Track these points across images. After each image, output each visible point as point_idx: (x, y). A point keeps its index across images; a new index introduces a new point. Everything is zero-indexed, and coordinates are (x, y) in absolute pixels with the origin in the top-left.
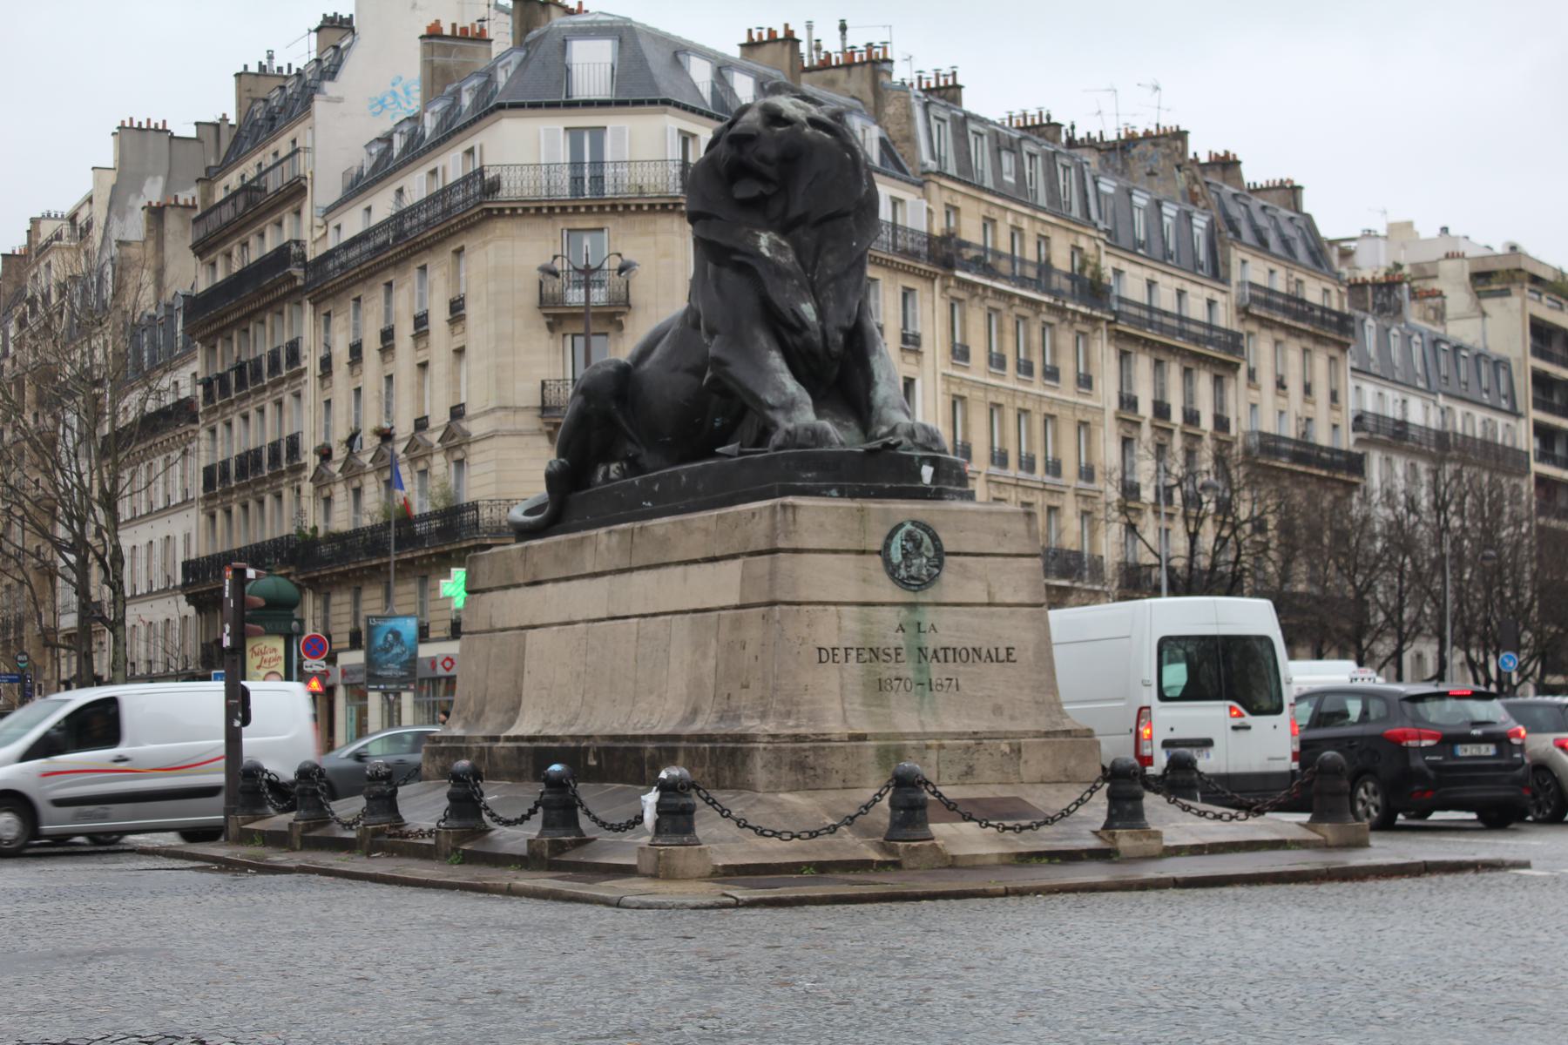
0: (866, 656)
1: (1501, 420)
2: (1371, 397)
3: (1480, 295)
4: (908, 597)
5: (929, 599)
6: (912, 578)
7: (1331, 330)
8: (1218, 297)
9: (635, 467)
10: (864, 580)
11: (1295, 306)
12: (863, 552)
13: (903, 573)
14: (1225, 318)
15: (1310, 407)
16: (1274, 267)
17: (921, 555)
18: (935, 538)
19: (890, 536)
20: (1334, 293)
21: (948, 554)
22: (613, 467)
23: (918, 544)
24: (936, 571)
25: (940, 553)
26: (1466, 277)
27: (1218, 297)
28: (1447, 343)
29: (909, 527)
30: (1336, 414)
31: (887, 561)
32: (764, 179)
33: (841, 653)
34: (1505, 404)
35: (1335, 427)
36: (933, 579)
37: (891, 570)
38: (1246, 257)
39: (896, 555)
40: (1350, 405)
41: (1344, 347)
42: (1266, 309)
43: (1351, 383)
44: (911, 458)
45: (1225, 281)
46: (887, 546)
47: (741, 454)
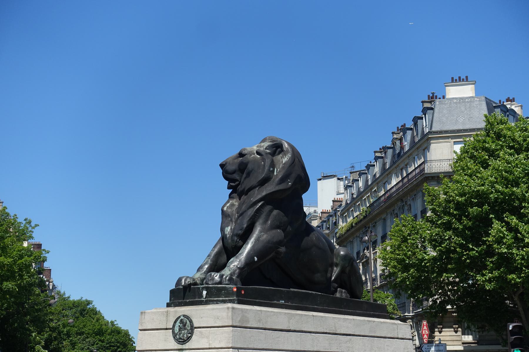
4: (180, 347)
5: (187, 348)
6: (180, 338)
10: (165, 341)
12: (167, 329)
13: (178, 336)
17: (185, 329)
18: (191, 321)
19: (175, 322)
21: (196, 328)
23: (185, 325)
24: (190, 335)
25: (193, 328)
29: (182, 317)
31: (173, 332)
36: (189, 339)
37: (174, 335)
39: (177, 329)
44: (199, 288)
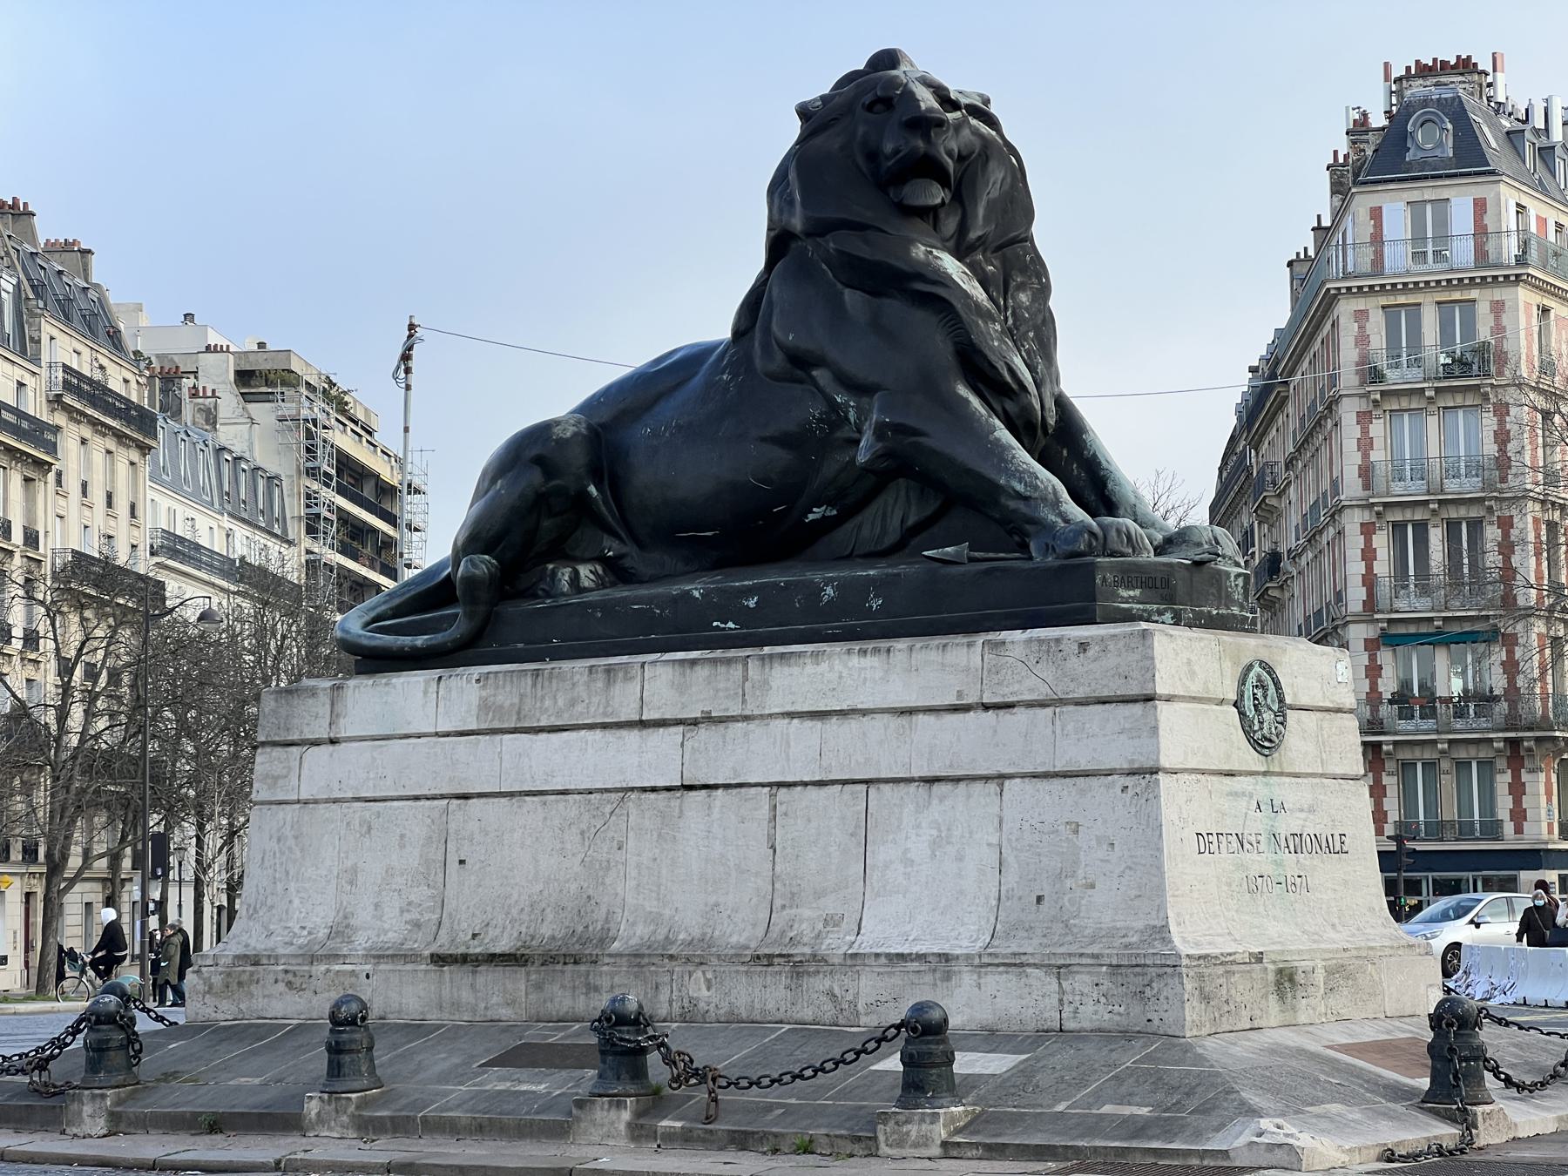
0: (1235, 844)
1: (275, 547)
2: (169, 511)
3: (247, 398)
7: (133, 425)
8: (28, 379)
9: (617, 572)
11: (97, 394)
14: (35, 406)
15: (112, 522)
16: (80, 347)
18: (1277, 684)
20: (133, 385)
22: (584, 571)
26: (232, 377)
27: (28, 379)
28: (231, 452)
29: (1257, 669)
30: (136, 532)
32: (944, 180)
33: (1213, 839)
34: (277, 530)
35: (133, 546)
38: (55, 332)
40: (147, 518)
41: (144, 449)
42: (84, 394)
43: (150, 494)
45: (36, 360)
46: (1241, 695)
47: (971, 560)
